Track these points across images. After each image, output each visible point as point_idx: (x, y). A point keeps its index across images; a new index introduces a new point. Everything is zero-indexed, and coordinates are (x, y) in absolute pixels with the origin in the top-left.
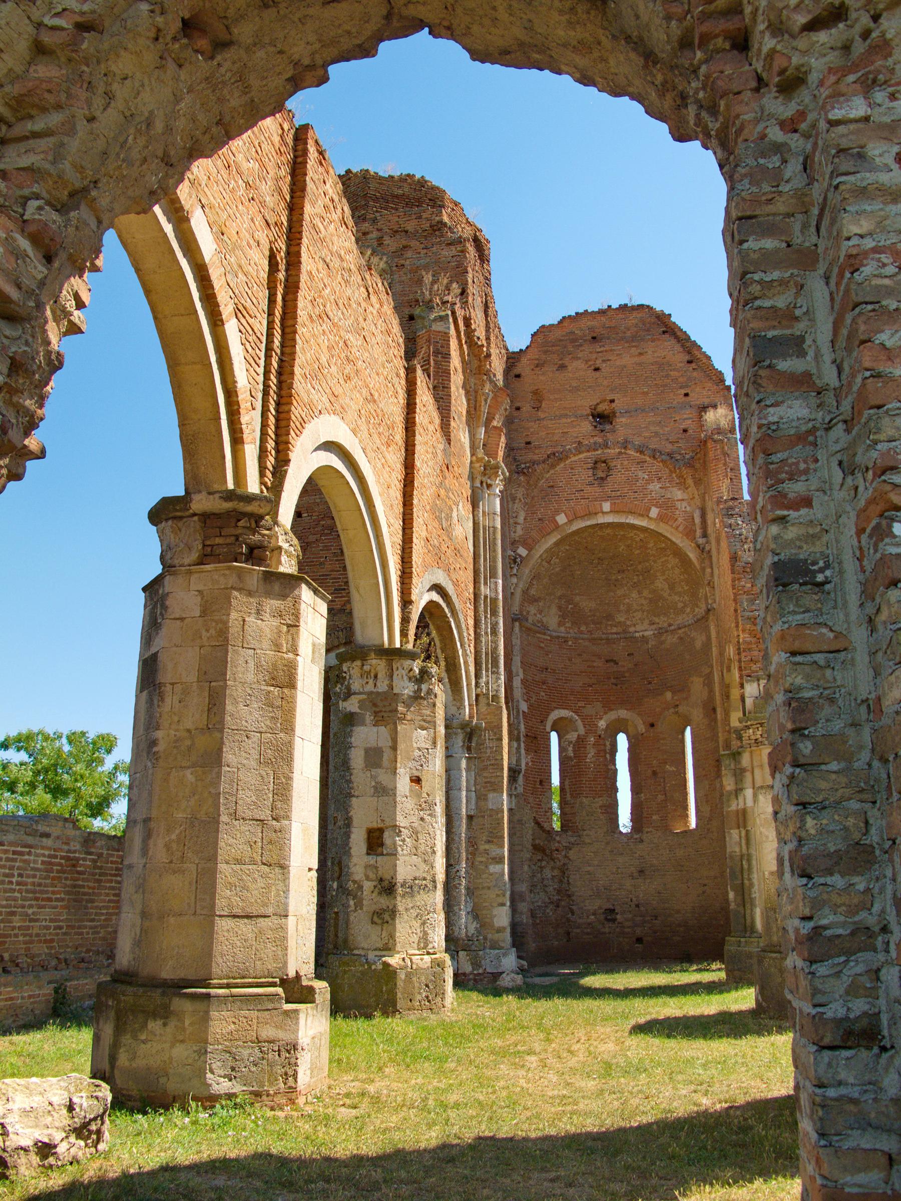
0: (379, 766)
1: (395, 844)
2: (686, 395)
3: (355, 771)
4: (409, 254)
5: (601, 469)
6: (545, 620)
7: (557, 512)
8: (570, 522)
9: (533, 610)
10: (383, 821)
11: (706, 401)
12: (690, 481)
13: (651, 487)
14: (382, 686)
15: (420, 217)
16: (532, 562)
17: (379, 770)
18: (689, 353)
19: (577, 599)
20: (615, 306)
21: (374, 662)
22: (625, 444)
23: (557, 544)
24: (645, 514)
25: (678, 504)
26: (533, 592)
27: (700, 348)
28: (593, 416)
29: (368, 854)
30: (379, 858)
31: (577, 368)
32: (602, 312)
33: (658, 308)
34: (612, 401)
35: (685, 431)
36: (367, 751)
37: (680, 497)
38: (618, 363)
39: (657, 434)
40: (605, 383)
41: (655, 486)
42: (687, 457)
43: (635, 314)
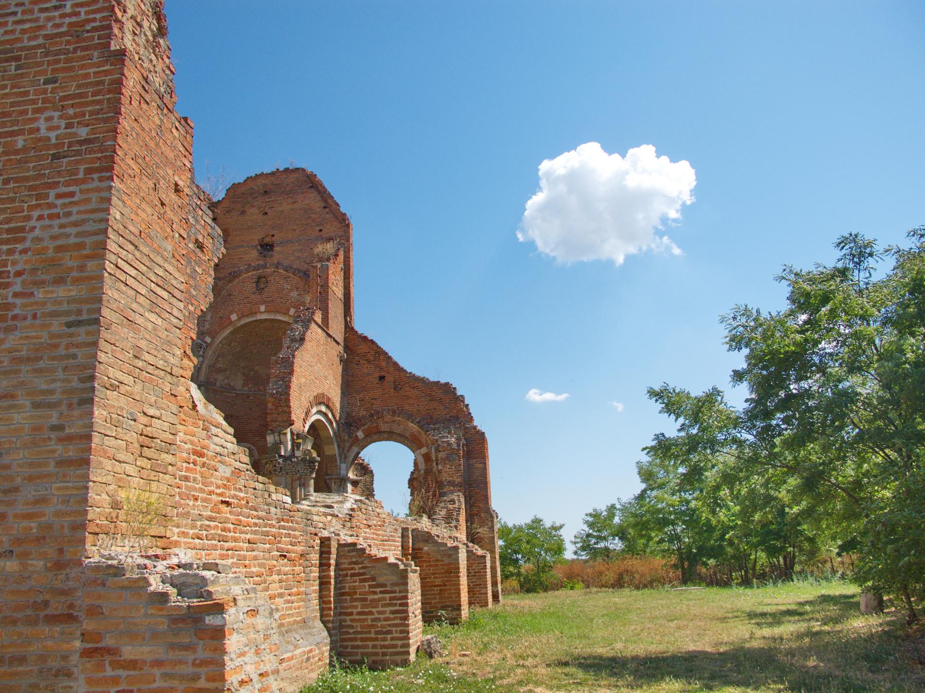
2: (321, 230)
5: (261, 282)
6: (232, 384)
7: (232, 312)
8: (239, 319)
9: (220, 377)
13: (292, 294)
16: (213, 347)
18: (326, 201)
19: (256, 368)
20: (281, 169)
22: (278, 265)
23: (232, 333)
24: (286, 313)
26: (219, 365)
28: (262, 246)
31: (253, 213)
32: (273, 174)
33: (309, 169)
34: (273, 236)
38: (279, 209)
39: (299, 258)
40: (270, 223)
41: (294, 294)
43: (295, 175)
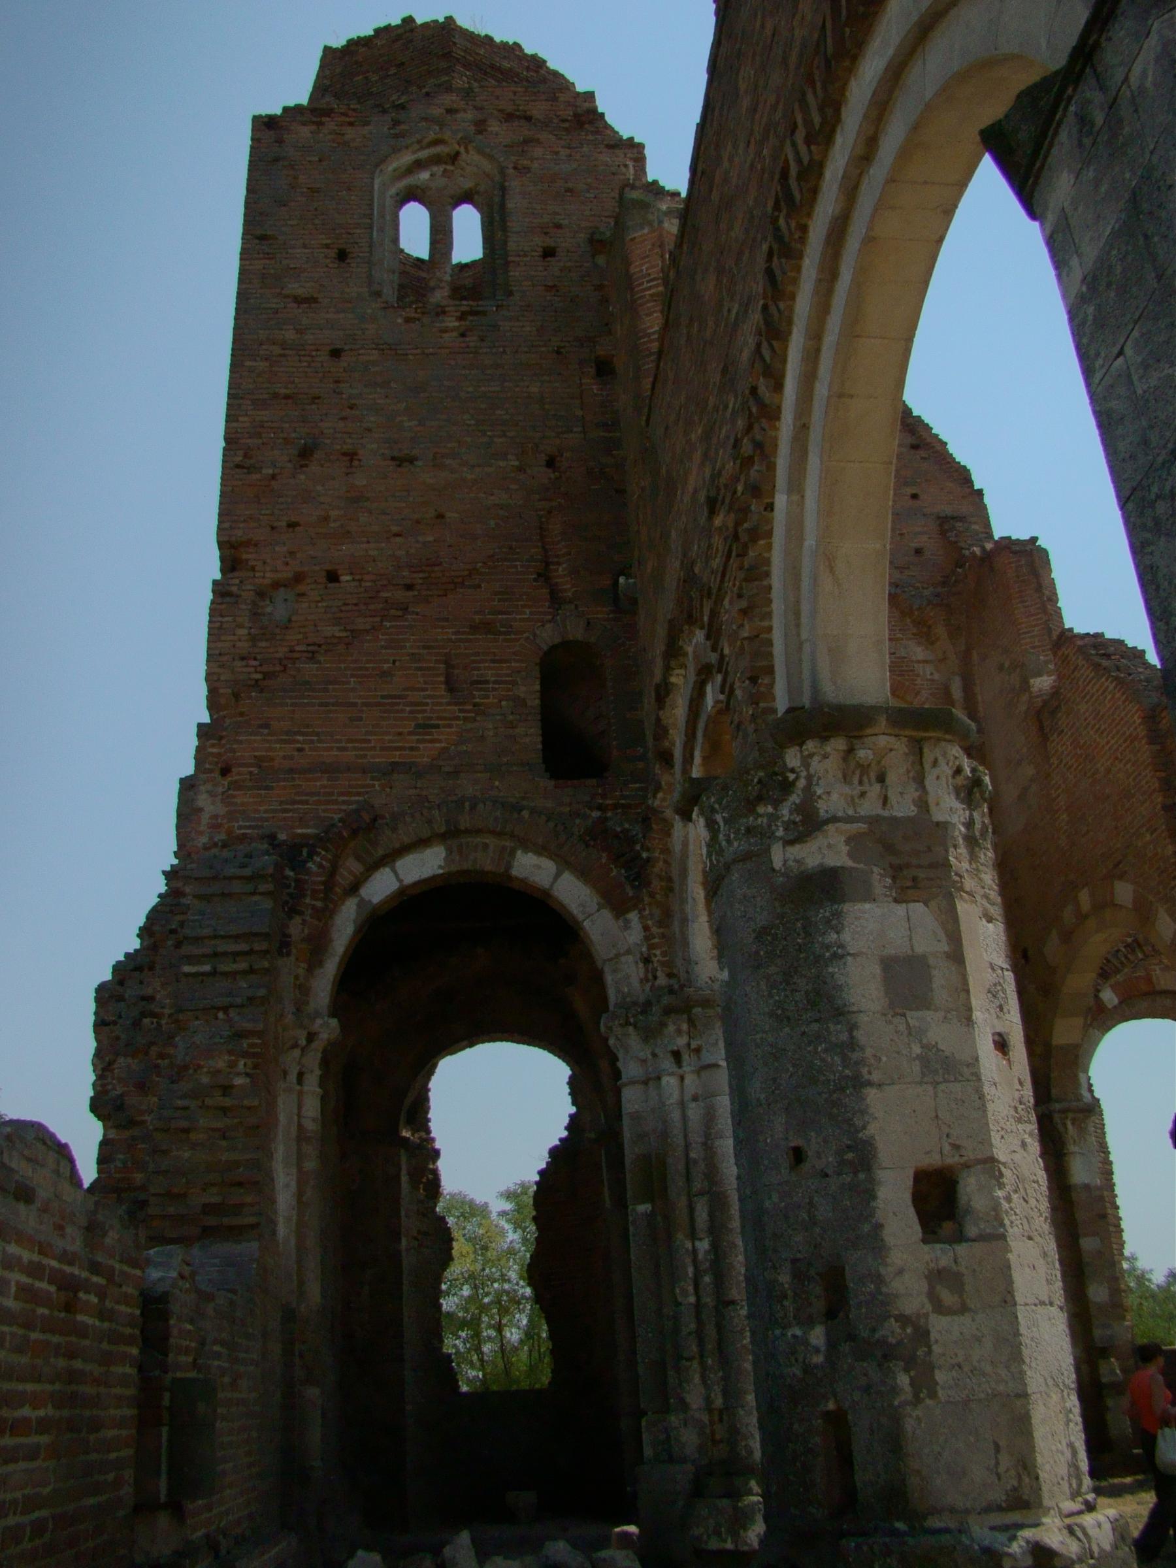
0: (923, 1001)
1: (996, 1207)
2: (914, 496)
3: (863, 1019)
4: (538, 152)
10: (956, 1147)
11: (948, 510)
12: (940, 631)
14: (903, 807)
15: (555, 99)
17: (928, 1015)
21: (883, 741)
25: (919, 668)
27: (928, 428)
29: (924, 1241)
30: (962, 1249)
35: (918, 552)
36: (889, 965)
37: (920, 657)
42: (926, 593)
